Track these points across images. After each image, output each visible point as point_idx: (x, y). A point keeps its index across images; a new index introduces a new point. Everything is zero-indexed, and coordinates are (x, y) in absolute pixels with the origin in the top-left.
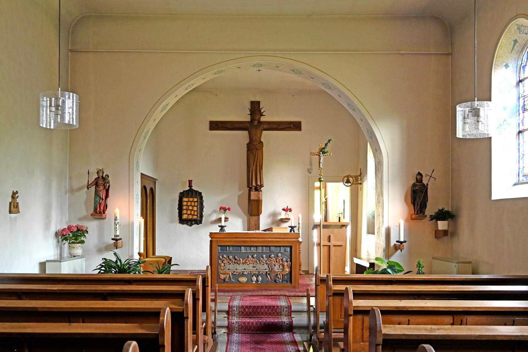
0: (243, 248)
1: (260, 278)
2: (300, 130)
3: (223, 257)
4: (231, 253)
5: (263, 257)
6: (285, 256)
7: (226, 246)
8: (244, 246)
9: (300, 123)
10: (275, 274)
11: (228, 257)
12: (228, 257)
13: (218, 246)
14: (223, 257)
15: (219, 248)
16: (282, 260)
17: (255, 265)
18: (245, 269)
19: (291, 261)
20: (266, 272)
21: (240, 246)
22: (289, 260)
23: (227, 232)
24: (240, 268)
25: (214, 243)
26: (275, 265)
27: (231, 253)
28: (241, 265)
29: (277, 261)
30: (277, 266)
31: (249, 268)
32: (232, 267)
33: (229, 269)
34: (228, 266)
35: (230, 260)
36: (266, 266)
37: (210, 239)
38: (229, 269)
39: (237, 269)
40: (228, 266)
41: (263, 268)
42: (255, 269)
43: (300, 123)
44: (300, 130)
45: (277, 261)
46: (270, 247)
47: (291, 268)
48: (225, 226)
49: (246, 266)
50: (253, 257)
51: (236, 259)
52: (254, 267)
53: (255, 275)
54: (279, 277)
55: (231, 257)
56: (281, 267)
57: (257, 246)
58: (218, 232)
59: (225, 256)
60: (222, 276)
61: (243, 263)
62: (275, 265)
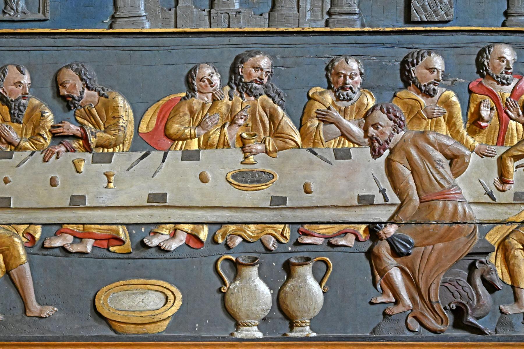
10: (463, 245)
17: (259, 162)
20: (373, 230)
24: (117, 188)
28: (120, 159)
31: (196, 192)
36: (367, 172)
39: (77, 202)
42: (260, 195)
49: (171, 175)
50: (235, 79)
52: (244, 178)
53: (259, 254)
61: (144, 144)
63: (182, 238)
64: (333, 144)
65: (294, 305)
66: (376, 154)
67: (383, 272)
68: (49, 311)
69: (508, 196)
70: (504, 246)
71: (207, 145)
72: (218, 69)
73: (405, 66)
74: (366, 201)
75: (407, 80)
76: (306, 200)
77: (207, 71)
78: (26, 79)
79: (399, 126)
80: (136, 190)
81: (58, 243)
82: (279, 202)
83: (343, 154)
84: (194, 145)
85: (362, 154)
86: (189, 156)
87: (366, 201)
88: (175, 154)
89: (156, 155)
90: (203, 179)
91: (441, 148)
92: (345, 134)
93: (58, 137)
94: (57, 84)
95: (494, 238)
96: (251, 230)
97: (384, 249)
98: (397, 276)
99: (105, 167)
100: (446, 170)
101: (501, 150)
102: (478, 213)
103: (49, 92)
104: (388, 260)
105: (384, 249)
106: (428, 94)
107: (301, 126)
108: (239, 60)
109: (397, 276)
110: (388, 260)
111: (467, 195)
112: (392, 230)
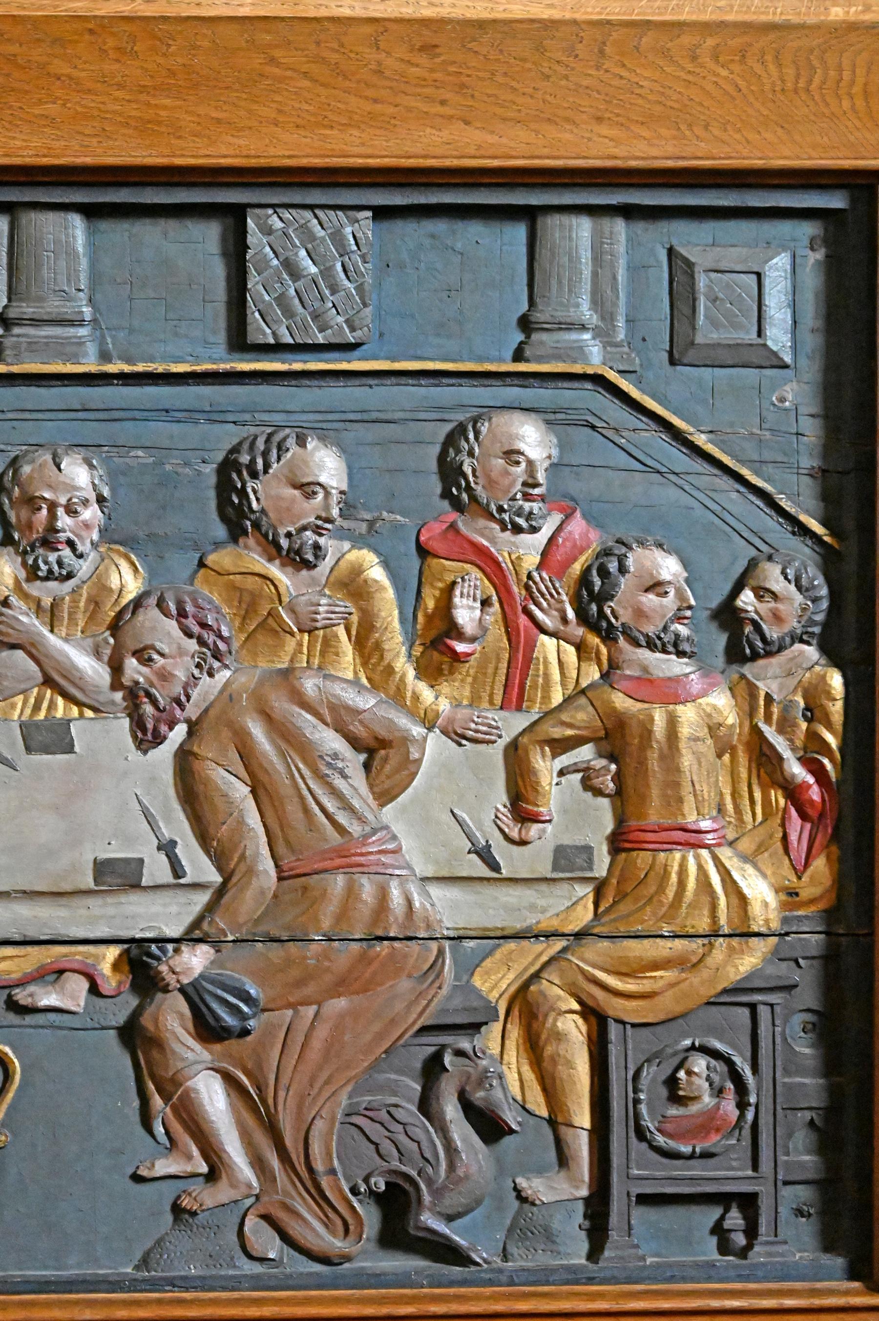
10: (406, 1003)
16: (592, 603)
20: (141, 963)
26: (378, 751)
29: (438, 646)
30: (450, 788)
36: (123, 791)
45: (438, 646)
54: (513, 1080)
56: (572, 809)
62: (378, 751)
64: (19, 709)
66: (147, 738)
67: (170, 1087)
69: (535, 859)
70: (526, 1006)
79: (213, 654)
87: (118, 876)
91: (340, 719)
92: (55, 680)
95: (495, 982)
97: (172, 1018)
98: (213, 1098)
100: (355, 784)
101: (514, 724)
102: (449, 909)
105: (172, 1018)
106: (298, 560)
109: (213, 1098)
112: (195, 961)
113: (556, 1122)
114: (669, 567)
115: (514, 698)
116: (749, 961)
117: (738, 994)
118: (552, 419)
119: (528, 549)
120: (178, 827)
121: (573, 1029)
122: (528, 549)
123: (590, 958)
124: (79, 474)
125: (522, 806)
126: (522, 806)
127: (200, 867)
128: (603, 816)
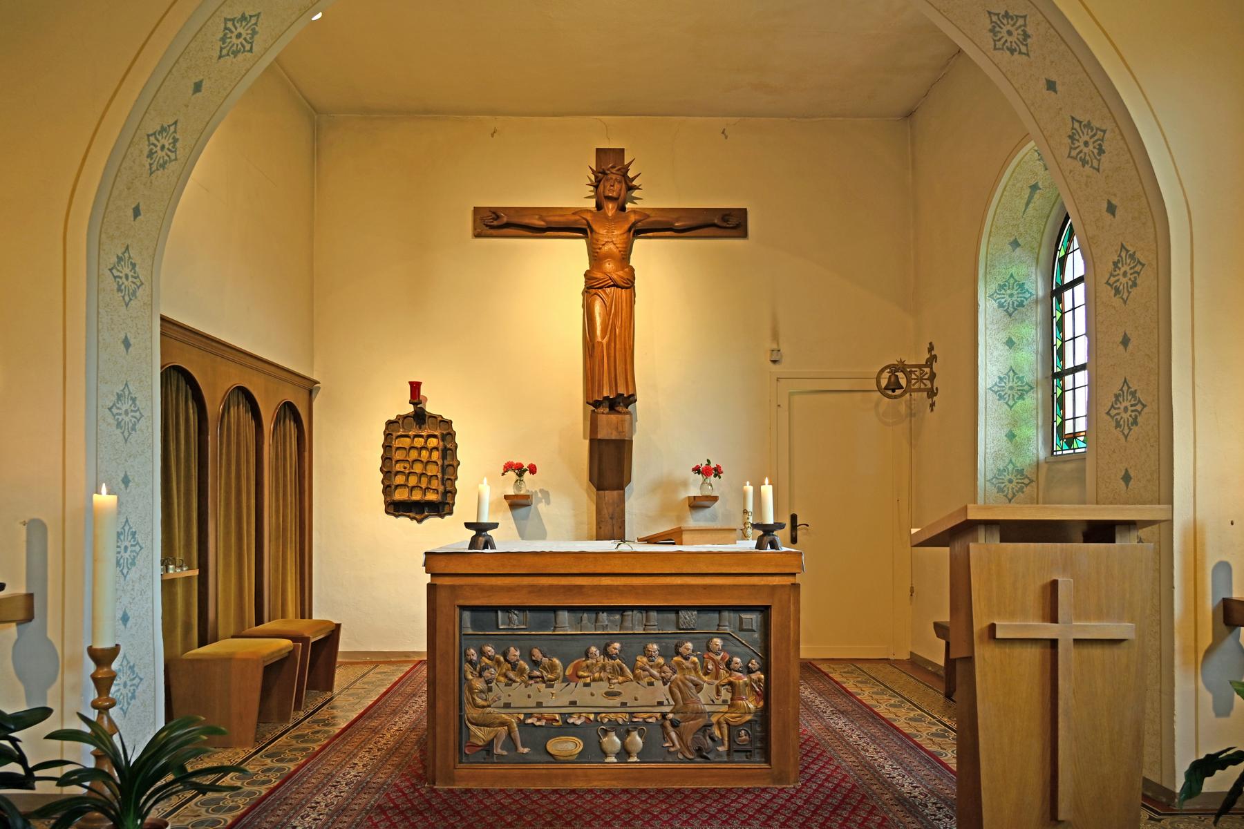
0: (564, 616)
1: (637, 740)
2: (744, 235)
3: (481, 653)
4: (514, 638)
5: (646, 653)
6: (741, 649)
7: (495, 609)
8: (571, 609)
9: (744, 212)
10: (701, 722)
11: (505, 655)
12: (505, 655)
13: (463, 608)
14: (481, 653)
15: (467, 615)
16: (728, 664)
17: (616, 688)
18: (573, 704)
19: (765, 668)
20: (664, 716)
21: (555, 609)
22: (754, 664)
23: (500, 548)
24: (556, 698)
25: (442, 597)
27: (514, 638)
28: (558, 685)
31: (589, 700)
32: (519, 694)
33: (507, 706)
34: (501, 691)
35: (514, 666)
36: (662, 692)
37: (427, 578)
38: (507, 706)
39: (539, 705)
40: (501, 691)
41: (649, 696)
42: (616, 701)
43: (744, 212)
44: (744, 235)
46: (676, 610)
47: (766, 695)
48: (495, 526)
49: (577, 692)
50: (605, 653)
51: (536, 664)
52: (610, 694)
53: (614, 726)
54: (717, 733)
55: (514, 653)
56: (726, 695)
57: (622, 610)
58: (464, 548)
59: (489, 649)
60: (481, 735)
61: (566, 680)
63: (583, 719)
64: (646, 680)
65: (630, 748)
66: (665, 684)
67: (668, 734)
68: (526, 750)
69: (720, 702)
70: (719, 723)
71: (594, 680)
72: (599, 648)
73: (677, 647)
74: (660, 704)
75: (678, 653)
76: (636, 703)
77: (593, 649)
78: (518, 653)
79: (675, 672)
80: (565, 700)
81: (529, 721)
82: (624, 704)
83: (651, 684)
84: (588, 680)
85: (658, 684)
86: (587, 685)
87: (660, 704)
88: (580, 683)
89: (573, 684)
90: (592, 695)
91: (692, 681)
92: (652, 675)
93: (531, 678)
94: (531, 655)
95: (714, 719)
96: (611, 716)
97: (668, 723)
98: (673, 735)
99: (551, 690)
100: (694, 691)
101: (717, 682)
102: (708, 708)
103: (527, 658)
104: (670, 728)
105: (668, 723)
106: (686, 659)
107: (633, 672)
108: (608, 645)
109: (673, 735)
110: (670, 728)
111: (703, 701)
112: (671, 716)
113: (722, 739)
114: (739, 660)
115: (717, 678)
116: (749, 717)
117: (749, 722)
118: (722, 639)
119: (719, 658)
120: (669, 697)
121: (725, 726)
122: (719, 658)
123: (727, 716)
124: (655, 647)
125: (718, 693)
126: (718, 693)
127: (672, 702)
128: (730, 695)
